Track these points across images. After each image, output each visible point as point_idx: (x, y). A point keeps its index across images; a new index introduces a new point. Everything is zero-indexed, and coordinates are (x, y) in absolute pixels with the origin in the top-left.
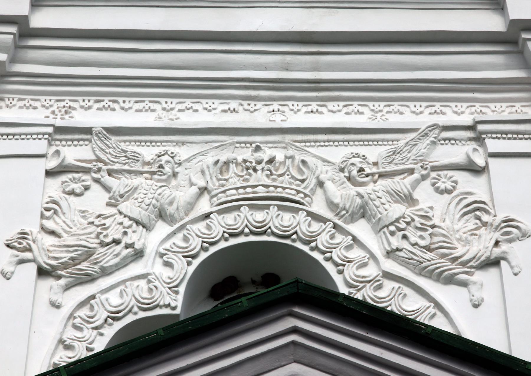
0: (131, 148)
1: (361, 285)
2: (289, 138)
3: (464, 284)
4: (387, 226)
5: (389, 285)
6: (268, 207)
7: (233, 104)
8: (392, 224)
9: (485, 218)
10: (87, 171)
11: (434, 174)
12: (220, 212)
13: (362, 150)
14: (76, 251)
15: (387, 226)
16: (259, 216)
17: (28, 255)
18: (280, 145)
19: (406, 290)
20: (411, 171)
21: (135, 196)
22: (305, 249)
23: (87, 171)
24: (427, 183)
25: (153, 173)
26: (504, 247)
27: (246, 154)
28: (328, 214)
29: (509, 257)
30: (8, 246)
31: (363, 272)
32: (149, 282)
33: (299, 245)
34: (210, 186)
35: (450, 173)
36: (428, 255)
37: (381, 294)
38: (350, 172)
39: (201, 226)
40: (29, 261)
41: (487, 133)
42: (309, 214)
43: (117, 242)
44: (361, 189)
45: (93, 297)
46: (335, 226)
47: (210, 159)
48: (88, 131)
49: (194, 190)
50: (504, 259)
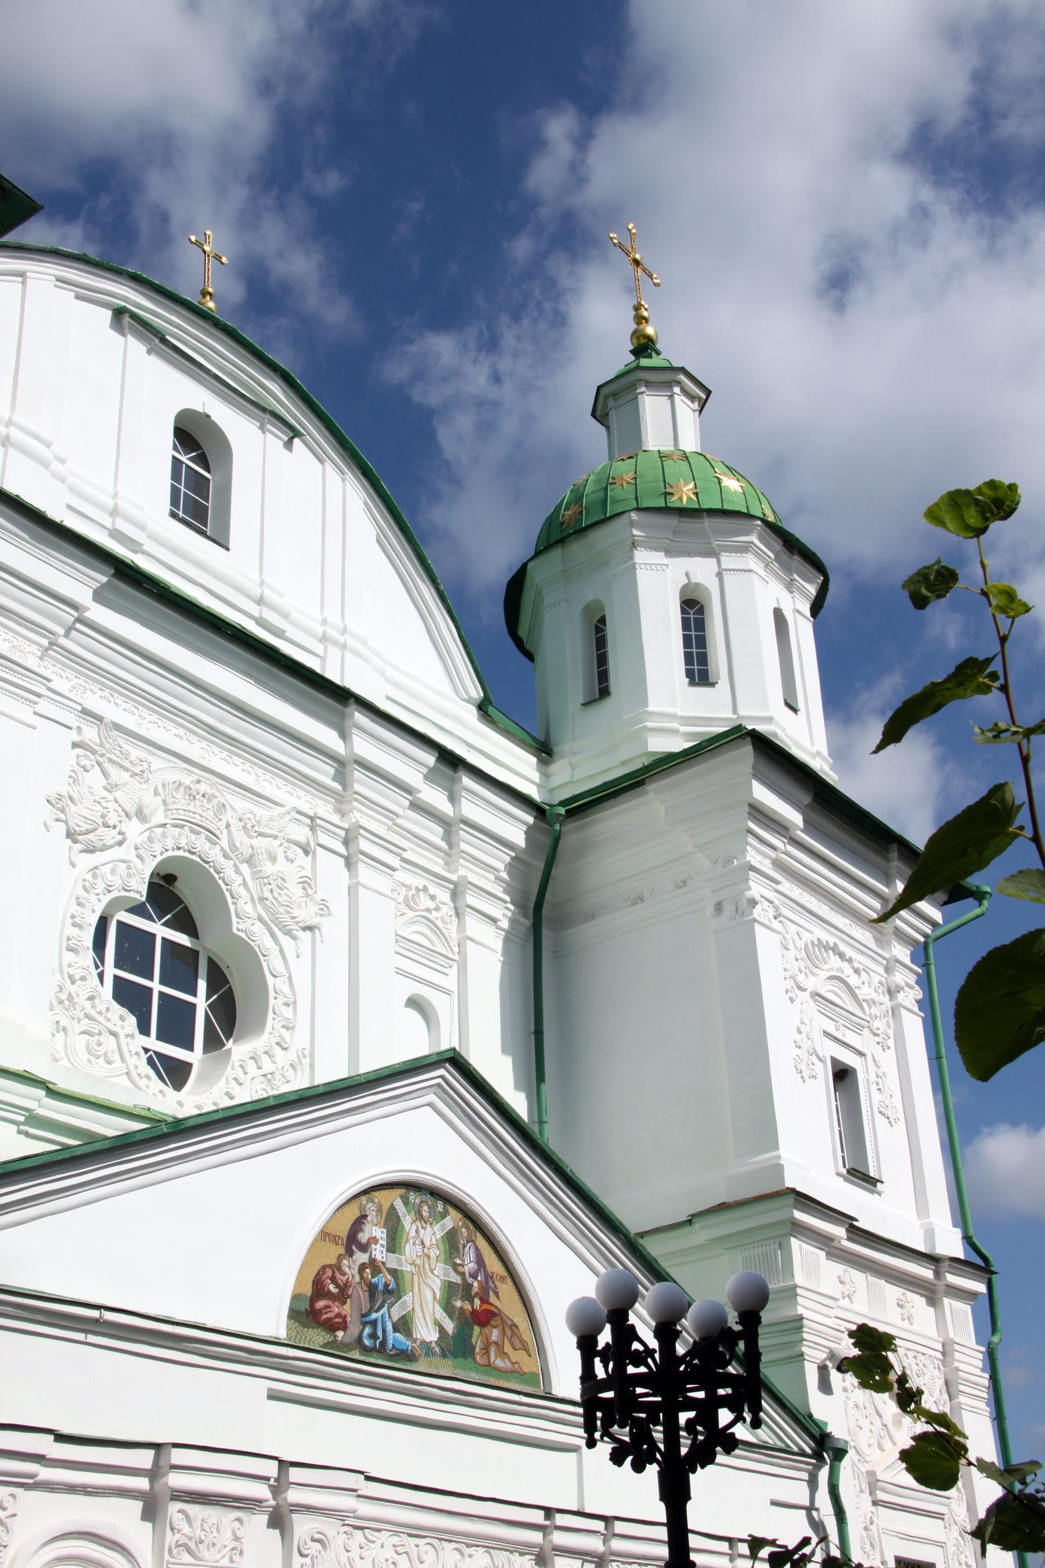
0: (125, 746)
1: (246, 919)
2: (214, 779)
3: (294, 938)
4: (263, 878)
6: (199, 833)
7: (181, 731)
8: (266, 878)
9: (310, 891)
10: (94, 752)
12: (175, 826)
13: (252, 807)
14: (91, 824)
15: (263, 878)
17: (62, 816)
18: (207, 782)
21: (124, 789)
23: (94, 752)
25: (137, 775)
29: (321, 928)
30: (48, 801)
32: (129, 868)
38: (245, 824)
40: (62, 821)
41: (319, 826)
43: (115, 827)
45: (96, 868)
48: (100, 719)
50: (318, 928)
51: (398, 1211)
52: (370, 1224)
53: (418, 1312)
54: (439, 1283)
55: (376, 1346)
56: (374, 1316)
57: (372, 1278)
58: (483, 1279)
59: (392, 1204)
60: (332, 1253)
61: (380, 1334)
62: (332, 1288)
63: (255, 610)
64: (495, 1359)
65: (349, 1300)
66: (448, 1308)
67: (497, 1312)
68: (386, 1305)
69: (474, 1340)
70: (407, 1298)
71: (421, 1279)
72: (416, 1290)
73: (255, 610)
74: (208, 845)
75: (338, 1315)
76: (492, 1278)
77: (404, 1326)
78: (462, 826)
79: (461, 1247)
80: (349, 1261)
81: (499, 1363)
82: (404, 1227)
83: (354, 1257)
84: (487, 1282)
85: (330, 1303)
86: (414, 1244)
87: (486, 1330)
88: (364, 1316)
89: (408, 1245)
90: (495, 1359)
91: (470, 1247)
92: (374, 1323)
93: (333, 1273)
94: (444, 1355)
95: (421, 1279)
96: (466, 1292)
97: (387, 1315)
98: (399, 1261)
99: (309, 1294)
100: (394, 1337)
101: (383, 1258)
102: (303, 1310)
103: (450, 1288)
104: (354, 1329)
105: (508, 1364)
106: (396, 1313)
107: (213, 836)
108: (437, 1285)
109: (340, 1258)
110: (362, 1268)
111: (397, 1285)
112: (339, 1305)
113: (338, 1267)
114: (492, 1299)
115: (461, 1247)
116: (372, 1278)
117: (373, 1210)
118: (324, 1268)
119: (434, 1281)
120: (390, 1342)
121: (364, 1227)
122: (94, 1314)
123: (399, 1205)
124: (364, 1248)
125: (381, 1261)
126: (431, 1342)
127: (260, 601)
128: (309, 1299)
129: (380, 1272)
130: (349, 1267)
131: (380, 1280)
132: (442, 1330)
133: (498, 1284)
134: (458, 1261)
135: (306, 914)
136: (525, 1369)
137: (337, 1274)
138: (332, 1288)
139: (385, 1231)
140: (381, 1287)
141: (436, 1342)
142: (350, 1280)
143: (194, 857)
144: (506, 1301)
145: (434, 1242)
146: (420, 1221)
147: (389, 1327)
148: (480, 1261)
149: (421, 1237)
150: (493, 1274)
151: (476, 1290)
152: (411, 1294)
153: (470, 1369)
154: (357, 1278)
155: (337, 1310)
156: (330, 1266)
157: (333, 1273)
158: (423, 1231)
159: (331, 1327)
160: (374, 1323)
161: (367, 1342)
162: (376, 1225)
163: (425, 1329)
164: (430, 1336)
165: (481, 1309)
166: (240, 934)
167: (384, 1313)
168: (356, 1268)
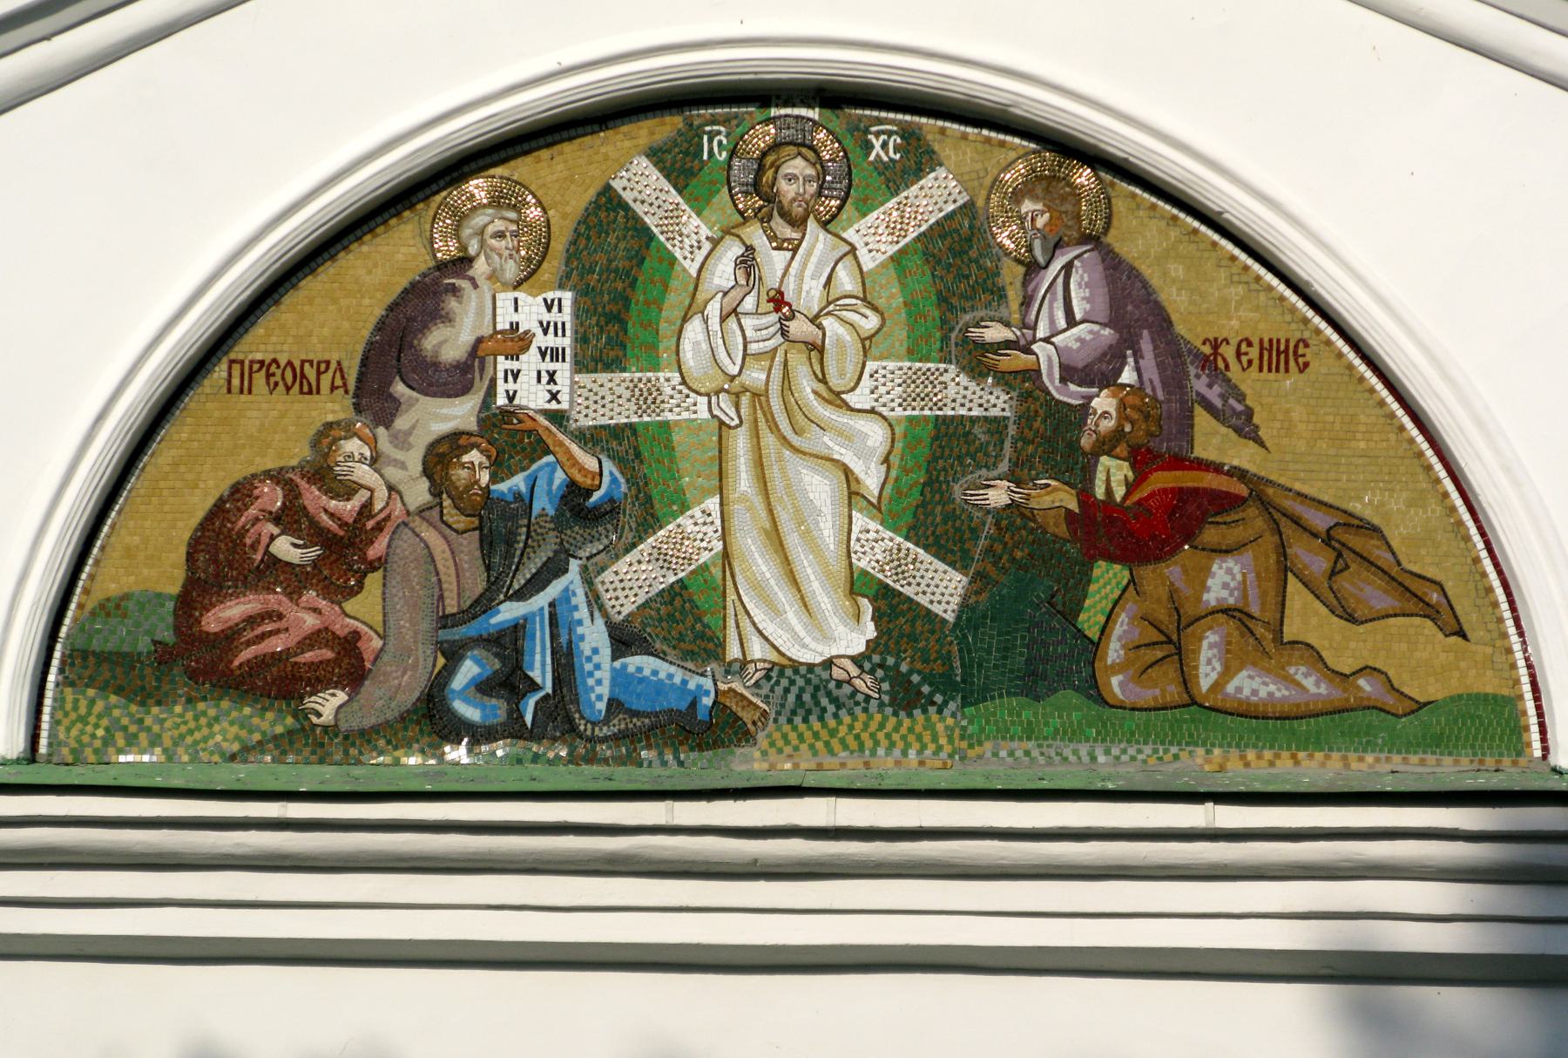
51: (639, 209)
52: (485, 286)
53: (756, 561)
54: (875, 435)
55: (521, 717)
56: (509, 612)
57: (494, 479)
58: (1151, 373)
59: (608, 189)
61: (540, 669)
62: (285, 548)
64: (1228, 672)
65: (373, 580)
67: (1242, 490)
68: (574, 565)
69: (1090, 620)
71: (769, 440)
72: (743, 481)
75: (314, 639)
76: (1210, 363)
79: (1011, 274)
80: (373, 443)
81: (1250, 685)
82: (672, 261)
83: (401, 423)
84: (1175, 381)
85: (276, 599)
86: (732, 312)
87: (1174, 570)
88: (445, 621)
89: (694, 329)
90: (1228, 672)
91: (1068, 268)
92: (510, 642)
93: (292, 492)
94: (905, 698)
95: (769, 440)
97: (580, 599)
98: (648, 398)
99: (175, 589)
100: (618, 677)
101: (554, 396)
102: (144, 645)
105: (1309, 683)
109: (327, 436)
112: (323, 604)
113: (323, 474)
115: (1011, 274)
116: (494, 479)
117: (500, 235)
118: (241, 492)
119: (846, 436)
120: (598, 687)
121: (452, 304)
125: (545, 413)
126: (829, 664)
128: (170, 605)
129: (541, 448)
130: (375, 461)
133: (1250, 382)
134: (995, 333)
136: (1431, 690)
137: (313, 498)
138: (285, 548)
139: (567, 297)
140: (543, 504)
141: (855, 660)
142: (378, 506)
145: (846, 281)
146: (766, 220)
147: (593, 636)
149: (772, 281)
150: (1216, 345)
151: (1108, 425)
152: (712, 503)
153: (1073, 734)
154: (418, 493)
155: (311, 622)
156: (277, 477)
157: (292, 492)
158: (780, 258)
160: (510, 642)
161: (469, 712)
162: (517, 285)
163: (793, 615)
164: (826, 636)
165: (1136, 497)
167: (567, 594)
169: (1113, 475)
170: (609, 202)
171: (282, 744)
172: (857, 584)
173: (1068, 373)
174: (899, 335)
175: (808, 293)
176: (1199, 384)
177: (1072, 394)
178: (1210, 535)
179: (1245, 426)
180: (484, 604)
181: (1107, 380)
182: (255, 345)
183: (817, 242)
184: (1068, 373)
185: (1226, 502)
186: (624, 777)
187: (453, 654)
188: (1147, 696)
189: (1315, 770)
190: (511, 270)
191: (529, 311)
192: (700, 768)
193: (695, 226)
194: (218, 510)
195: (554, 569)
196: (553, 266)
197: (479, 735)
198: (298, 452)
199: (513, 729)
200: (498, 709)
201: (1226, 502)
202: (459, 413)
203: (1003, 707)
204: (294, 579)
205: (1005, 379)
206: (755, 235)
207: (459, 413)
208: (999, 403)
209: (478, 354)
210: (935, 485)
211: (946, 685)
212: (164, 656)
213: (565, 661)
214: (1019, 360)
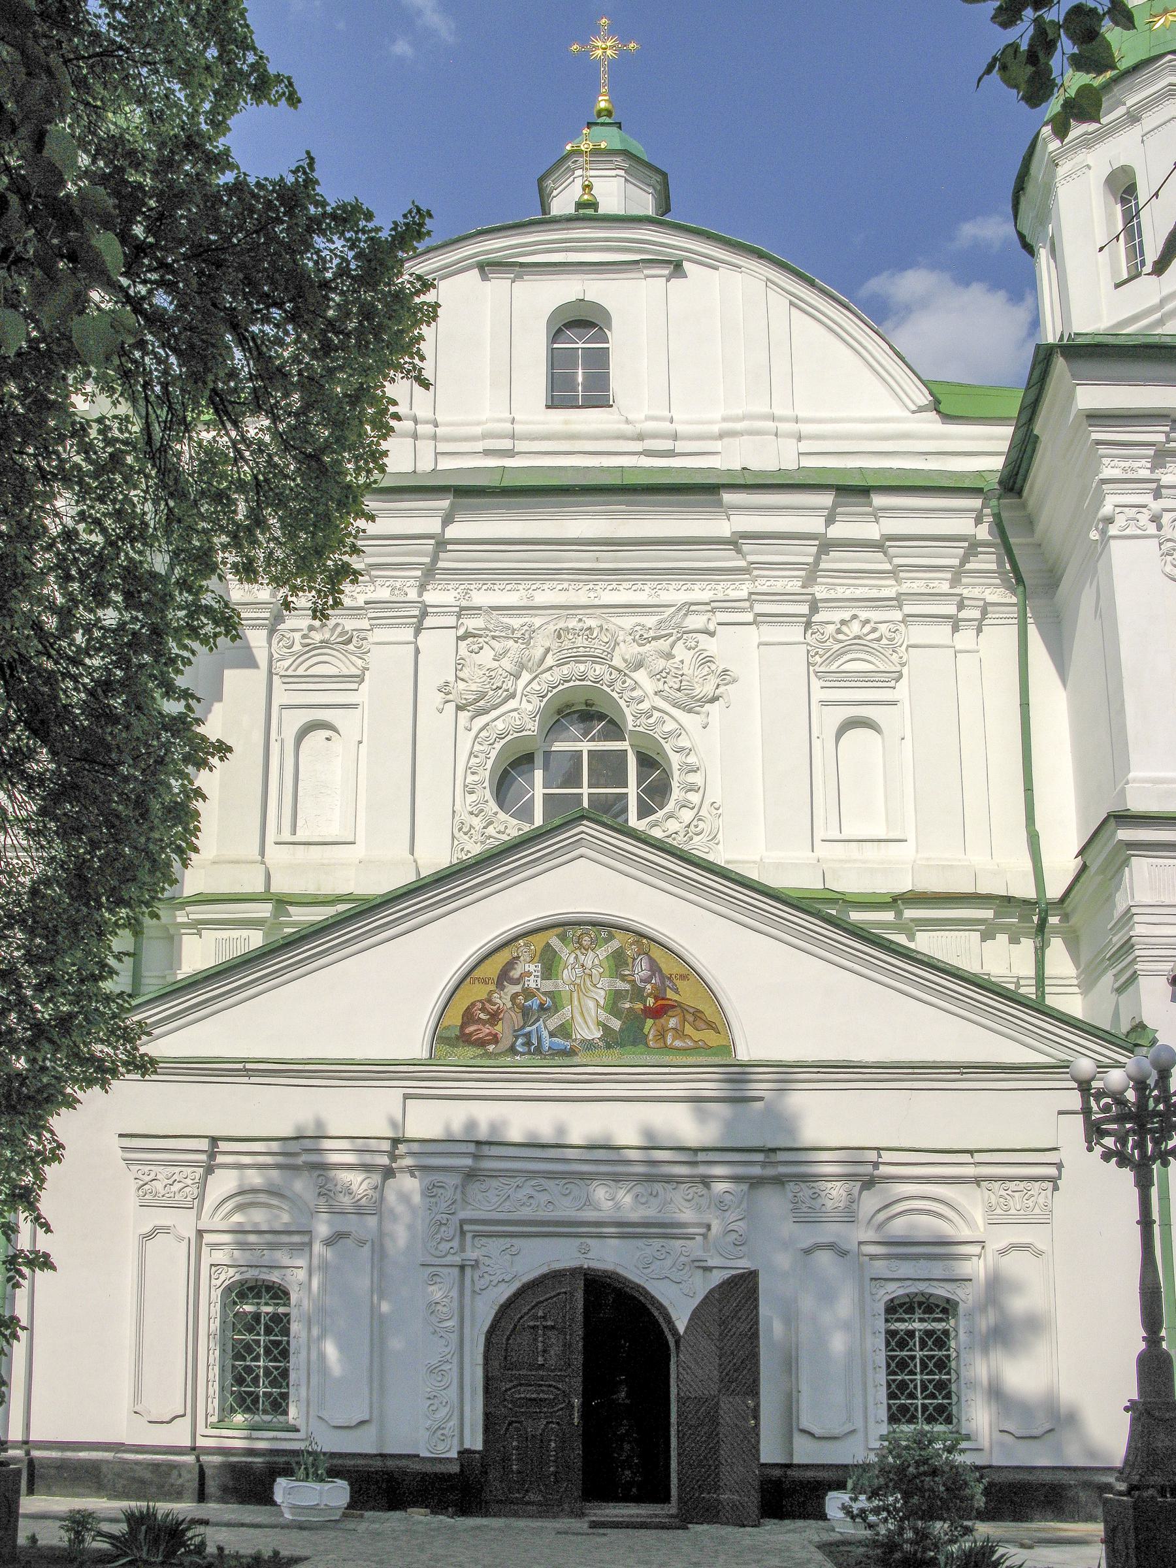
5: (656, 714)
7: (566, 585)
9: (713, 667)
11: (685, 636)
16: (582, 667)
19: (666, 717)
20: (671, 635)
22: (608, 690)
24: (680, 643)
26: (721, 689)
27: (572, 623)
28: (621, 665)
31: (641, 706)
33: (605, 688)
34: (552, 647)
35: (695, 635)
36: (679, 694)
37: (651, 721)
39: (547, 675)
42: (610, 666)
44: (641, 649)
46: (625, 675)
47: (552, 628)
49: (541, 651)
54: (603, 993)
56: (528, 1029)
60: (478, 992)
61: (535, 1041)
62: (482, 1016)
63: (638, 446)
66: (614, 1010)
69: (646, 1031)
70: (566, 1011)
72: (576, 1003)
73: (638, 446)
74: (598, 667)
75: (489, 1034)
77: (564, 1031)
78: (888, 543)
79: (630, 960)
81: (678, 1043)
84: (663, 983)
85: (480, 1027)
87: (662, 1020)
88: (515, 1031)
89: (566, 971)
92: (528, 1035)
94: (609, 1046)
96: (637, 993)
98: (557, 986)
103: (617, 995)
104: (505, 1044)
106: (553, 1022)
107: (596, 659)
108: (601, 996)
109: (491, 993)
110: (514, 997)
111: (554, 1003)
113: (490, 1001)
114: (670, 994)
115: (630, 960)
118: (473, 1004)
119: (597, 993)
122: (240, 1066)
123: (555, 942)
124: (516, 982)
127: (640, 437)
131: (534, 1003)
132: (606, 1028)
133: (678, 982)
134: (627, 972)
135: (708, 689)
137: (488, 1005)
138: (482, 1016)
140: (535, 1007)
143: (571, 684)
144: (685, 995)
145: (596, 962)
147: (545, 1034)
148: (654, 967)
153: (642, 1054)
154: (509, 1005)
156: (480, 1001)
159: (482, 1043)
160: (528, 1035)
161: (520, 1050)
166: (637, 729)
168: (509, 998)
169: (650, 1001)
170: (548, 945)
171: (482, 1056)
172: (599, 1023)
173: (641, 981)
174: (607, 973)
175: (589, 964)
176: (668, 983)
177: (642, 985)
178: (670, 1013)
179: (677, 991)
180: (523, 1027)
181: (650, 982)
182: (476, 974)
183: (591, 954)
184: (641, 981)
185: (673, 1007)
186: (551, 1063)
187: (517, 1037)
188: (658, 1045)
189: (691, 1060)
190: (528, 959)
191: (532, 968)
192: (567, 1061)
193: (566, 951)
194: (468, 1008)
195: (537, 1020)
196: (537, 959)
197: (523, 1054)
198: (485, 996)
199: (529, 1053)
200: (526, 1049)
201: (673, 1007)
202: (517, 988)
203: (628, 1048)
204: (484, 1022)
205: (629, 982)
206: (578, 952)
207: (517, 988)
208: (628, 987)
209: (521, 976)
210: (615, 1003)
211: (617, 1044)
212: (457, 1038)
213: (539, 1039)
214: (632, 978)
